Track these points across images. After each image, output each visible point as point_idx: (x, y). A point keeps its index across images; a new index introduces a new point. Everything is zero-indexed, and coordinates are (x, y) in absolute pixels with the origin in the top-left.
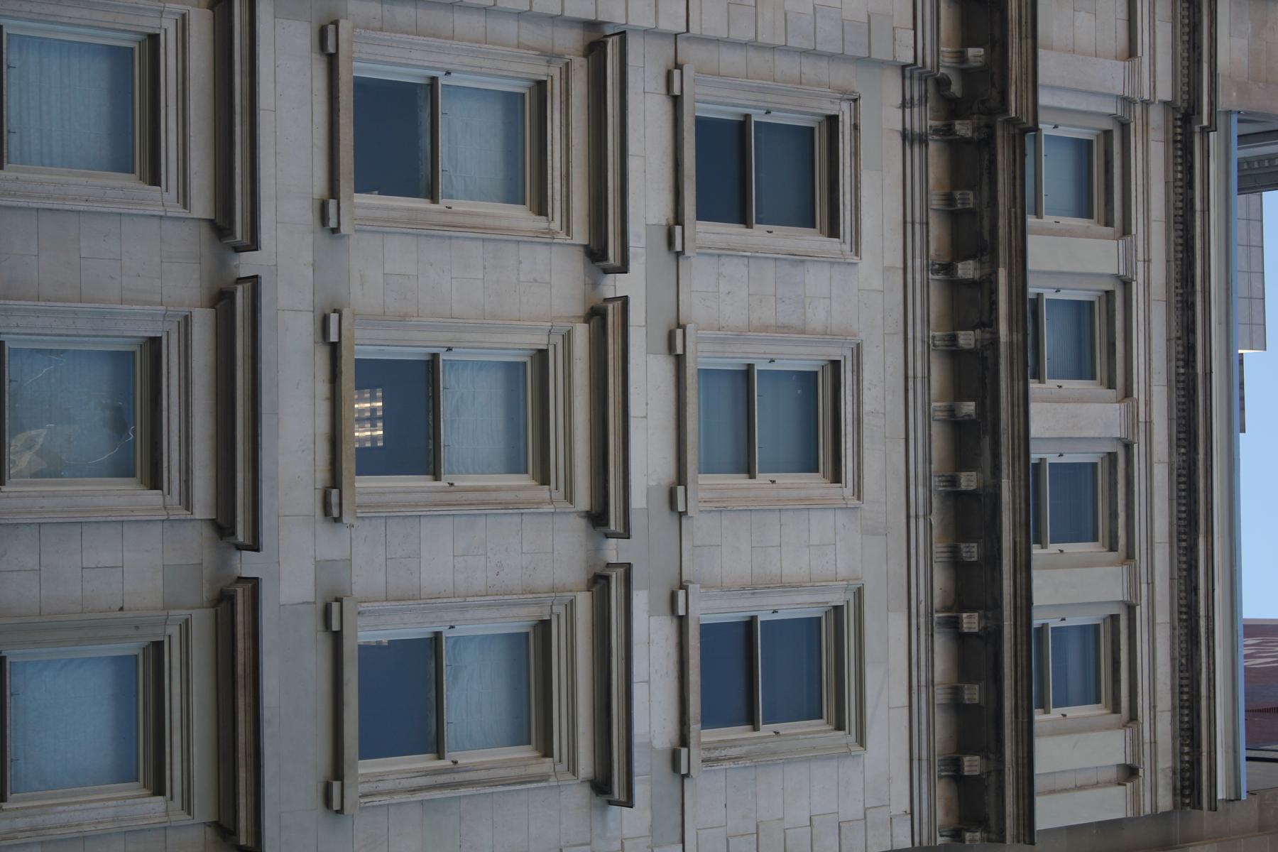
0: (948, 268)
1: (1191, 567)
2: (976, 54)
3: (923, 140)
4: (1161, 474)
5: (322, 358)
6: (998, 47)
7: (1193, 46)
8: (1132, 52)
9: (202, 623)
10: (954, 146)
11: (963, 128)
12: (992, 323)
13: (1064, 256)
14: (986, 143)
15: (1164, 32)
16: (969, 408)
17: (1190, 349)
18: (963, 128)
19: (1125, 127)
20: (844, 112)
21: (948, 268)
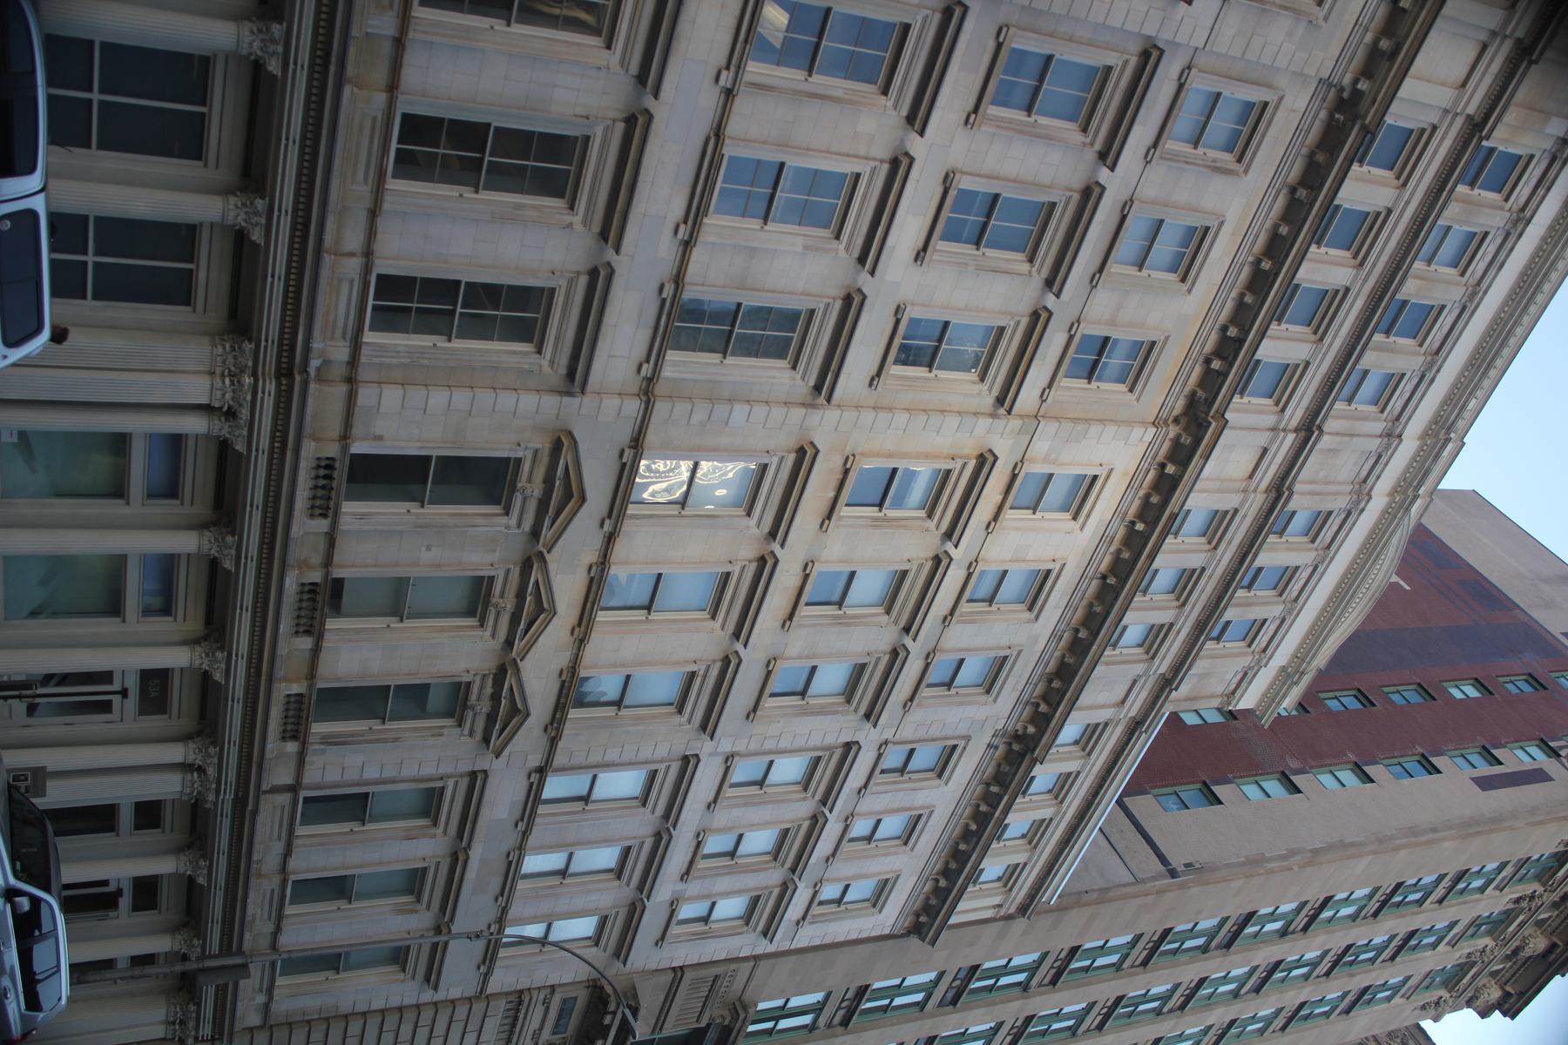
0: (988, 784)
1: (1060, 854)
2: (1031, 730)
3: (996, 748)
4: (1063, 825)
5: (694, 843)
6: (1041, 732)
7: (1154, 703)
8: (1123, 702)
9: (623, 913)
10: (1010, 751)
11: (1016, 747)
12: (995, 808)
13: (1281, 345)
14: (1022, 756)
15: (1144, 694)
16: (974, 827)
17: (1097, 793)
18: (1016, 747)
19: (1106, 724)
20: (962, 743)
21: (988, 784)
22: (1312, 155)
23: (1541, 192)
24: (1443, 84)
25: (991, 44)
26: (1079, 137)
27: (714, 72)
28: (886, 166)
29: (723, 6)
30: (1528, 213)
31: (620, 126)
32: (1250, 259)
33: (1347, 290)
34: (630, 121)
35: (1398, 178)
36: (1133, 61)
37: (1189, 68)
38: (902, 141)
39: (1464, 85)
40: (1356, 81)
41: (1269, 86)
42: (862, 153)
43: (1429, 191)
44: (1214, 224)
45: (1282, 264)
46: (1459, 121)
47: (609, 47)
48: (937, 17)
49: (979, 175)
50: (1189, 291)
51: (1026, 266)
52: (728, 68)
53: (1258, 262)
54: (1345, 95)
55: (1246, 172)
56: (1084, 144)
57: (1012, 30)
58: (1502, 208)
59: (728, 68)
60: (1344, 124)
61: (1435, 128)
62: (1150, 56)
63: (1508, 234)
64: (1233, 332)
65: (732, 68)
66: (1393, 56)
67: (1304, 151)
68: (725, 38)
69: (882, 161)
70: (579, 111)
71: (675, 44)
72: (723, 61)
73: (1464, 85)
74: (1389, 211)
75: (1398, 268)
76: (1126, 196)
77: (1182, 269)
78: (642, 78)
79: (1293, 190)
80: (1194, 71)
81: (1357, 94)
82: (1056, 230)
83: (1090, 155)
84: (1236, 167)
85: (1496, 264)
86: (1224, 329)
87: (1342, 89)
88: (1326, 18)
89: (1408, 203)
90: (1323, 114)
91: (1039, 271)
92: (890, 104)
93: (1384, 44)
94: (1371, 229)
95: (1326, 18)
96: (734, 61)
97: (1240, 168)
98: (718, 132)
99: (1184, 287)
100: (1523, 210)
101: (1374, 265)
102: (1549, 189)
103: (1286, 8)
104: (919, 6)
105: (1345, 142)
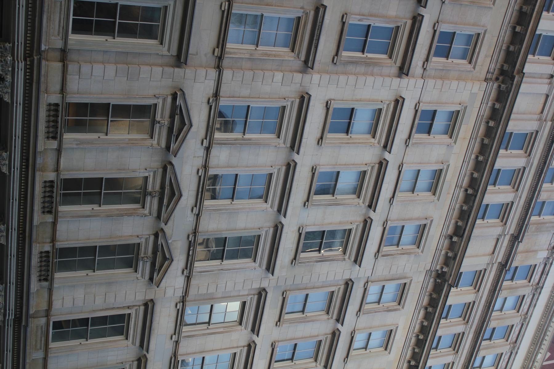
22: (431, 295)
23: (544, 276)
24: (484, 255)
25: (281, 299)
26: (326, 317)
27: (170, 336)
28: (246, 348)
29: (169, 315)
30: (541, 285)
31: (136, 363)
32: (414, 335)
33: (464, 333)
34: (139, 360)
35: (475, 289)
36: (342, 287)
37: (367, 282)
38: (251, 338)
39: (493, 253)
40: (442, 268)
41: (405, 278)
42: (235, 345)
43: (490, 291)
44: (393, 328)
45: (428, 337)
46: (495, 266)
47: (127, 339)
48: (256, 297)
49: (286, 340)
50: (389, 353)
51: (314, 364)
52: (175, 334)
53: (418, 336)
54: (439, 272)
55: (403, 308)
56: (328, 319)
57: (288, 292)
58: (528, 286)
59: (175, 334)
60: (441, 283)
61: (485, 270)
62: (348, 285)
63: (534, 295)
64: (413, 363)
65: (177, 334)
66: (455, 258)
67: (427, 294)
68: (172, 325)
69: (244, 347)
70: (118, 361)
71: (152, 332)
72: (173, 332)
73: (493, 253)
74: (474, 302)
75: (484, 321)
76: (352, 329)
77: (384, 345)
78: (141, 345)
79: (426, 308)
80: (369, 283)
81: (444, 273)
82: (324, 349)
83: (332, 321)
84: (398, 307)
85: (532, 305)
86: (409, 362)
87: (438, 270)
88: (422, 252)
89: (481, 297)
90: (432, 280)
91: (320, 364)
92: (243, 328)
93: (450, 254)
94: (468, 308)
95: (422, 252)
96: (177, 332)
97: (400, 307)
98: (175, 354)
99: (387, 352)
100: (538, 284)
101: (473, 322)
102: (547, 275)
103: (403, 254)
104: (248, 295)
105: (443, 290)
